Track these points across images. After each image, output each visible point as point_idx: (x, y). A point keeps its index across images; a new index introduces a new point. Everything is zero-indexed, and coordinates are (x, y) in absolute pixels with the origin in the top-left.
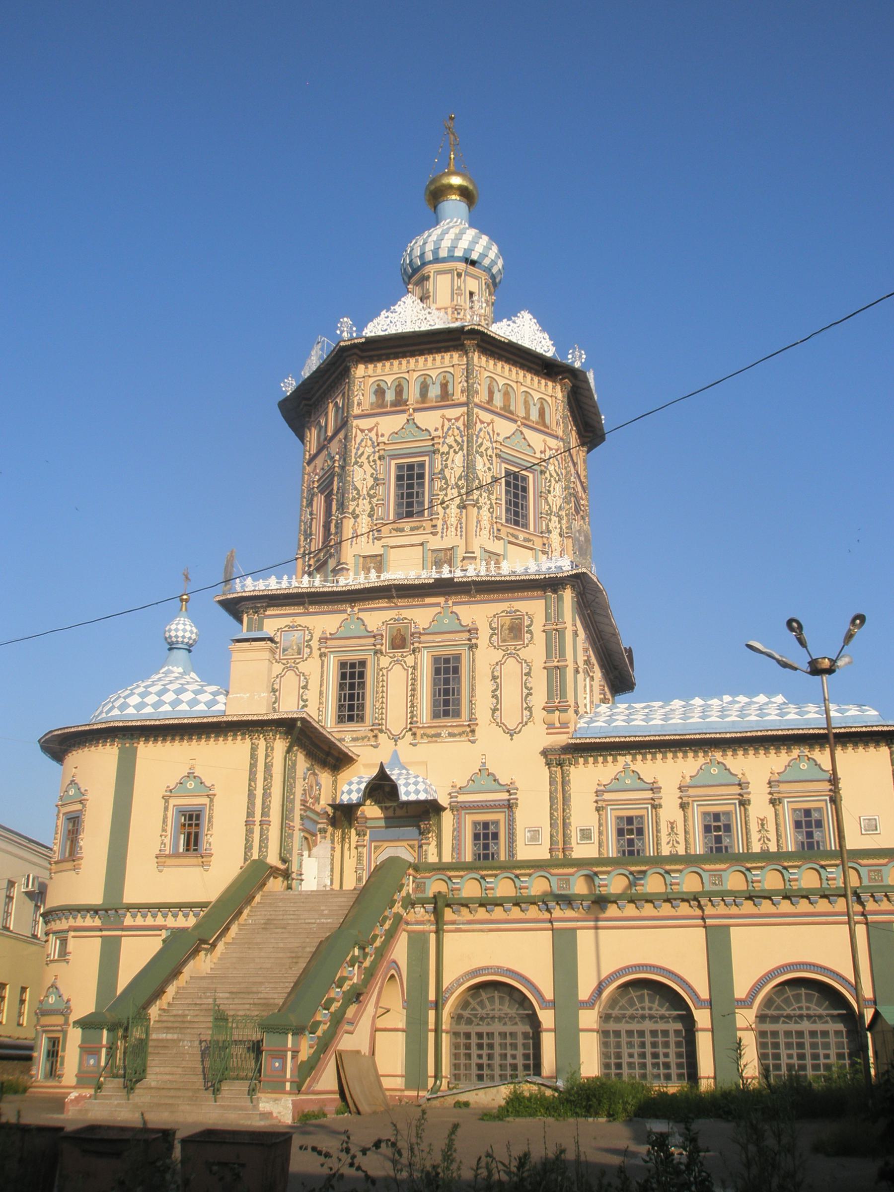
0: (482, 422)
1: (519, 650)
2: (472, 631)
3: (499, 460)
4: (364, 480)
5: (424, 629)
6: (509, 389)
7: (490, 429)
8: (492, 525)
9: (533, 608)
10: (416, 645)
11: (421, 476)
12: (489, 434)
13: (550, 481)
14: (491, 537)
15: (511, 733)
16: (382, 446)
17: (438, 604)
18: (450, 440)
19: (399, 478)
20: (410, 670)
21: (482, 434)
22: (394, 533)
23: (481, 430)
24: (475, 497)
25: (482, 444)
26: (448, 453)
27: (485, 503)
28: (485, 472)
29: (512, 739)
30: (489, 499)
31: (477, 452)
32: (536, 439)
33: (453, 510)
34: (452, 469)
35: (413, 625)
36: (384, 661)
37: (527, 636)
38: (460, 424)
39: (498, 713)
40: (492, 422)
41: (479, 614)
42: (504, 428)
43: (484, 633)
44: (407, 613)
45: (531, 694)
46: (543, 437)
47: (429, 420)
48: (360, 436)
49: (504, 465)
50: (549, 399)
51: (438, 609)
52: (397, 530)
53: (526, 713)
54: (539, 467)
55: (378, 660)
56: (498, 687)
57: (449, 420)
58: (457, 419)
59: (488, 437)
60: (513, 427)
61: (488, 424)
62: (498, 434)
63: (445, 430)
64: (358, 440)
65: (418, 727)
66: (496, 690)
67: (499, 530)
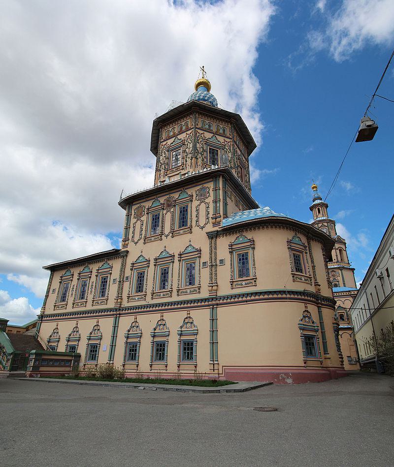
6: (211, 124)
8: (203, 164)
17: (181, 190)
32: (221, 139)
33: (189, 161)
36: (165, 212)
38: (191, 135)
41: (192, 191)
42: (208, 135)
43: (195, 196)
44: (172, 195)
47: (182, 136)
49: (209, 147)
51: (180, 192)
53: (207, 220)
54: (223, 147)
56: (198, 213)
58: (191, 133)
61: (202, 134)
67: (205, 166)
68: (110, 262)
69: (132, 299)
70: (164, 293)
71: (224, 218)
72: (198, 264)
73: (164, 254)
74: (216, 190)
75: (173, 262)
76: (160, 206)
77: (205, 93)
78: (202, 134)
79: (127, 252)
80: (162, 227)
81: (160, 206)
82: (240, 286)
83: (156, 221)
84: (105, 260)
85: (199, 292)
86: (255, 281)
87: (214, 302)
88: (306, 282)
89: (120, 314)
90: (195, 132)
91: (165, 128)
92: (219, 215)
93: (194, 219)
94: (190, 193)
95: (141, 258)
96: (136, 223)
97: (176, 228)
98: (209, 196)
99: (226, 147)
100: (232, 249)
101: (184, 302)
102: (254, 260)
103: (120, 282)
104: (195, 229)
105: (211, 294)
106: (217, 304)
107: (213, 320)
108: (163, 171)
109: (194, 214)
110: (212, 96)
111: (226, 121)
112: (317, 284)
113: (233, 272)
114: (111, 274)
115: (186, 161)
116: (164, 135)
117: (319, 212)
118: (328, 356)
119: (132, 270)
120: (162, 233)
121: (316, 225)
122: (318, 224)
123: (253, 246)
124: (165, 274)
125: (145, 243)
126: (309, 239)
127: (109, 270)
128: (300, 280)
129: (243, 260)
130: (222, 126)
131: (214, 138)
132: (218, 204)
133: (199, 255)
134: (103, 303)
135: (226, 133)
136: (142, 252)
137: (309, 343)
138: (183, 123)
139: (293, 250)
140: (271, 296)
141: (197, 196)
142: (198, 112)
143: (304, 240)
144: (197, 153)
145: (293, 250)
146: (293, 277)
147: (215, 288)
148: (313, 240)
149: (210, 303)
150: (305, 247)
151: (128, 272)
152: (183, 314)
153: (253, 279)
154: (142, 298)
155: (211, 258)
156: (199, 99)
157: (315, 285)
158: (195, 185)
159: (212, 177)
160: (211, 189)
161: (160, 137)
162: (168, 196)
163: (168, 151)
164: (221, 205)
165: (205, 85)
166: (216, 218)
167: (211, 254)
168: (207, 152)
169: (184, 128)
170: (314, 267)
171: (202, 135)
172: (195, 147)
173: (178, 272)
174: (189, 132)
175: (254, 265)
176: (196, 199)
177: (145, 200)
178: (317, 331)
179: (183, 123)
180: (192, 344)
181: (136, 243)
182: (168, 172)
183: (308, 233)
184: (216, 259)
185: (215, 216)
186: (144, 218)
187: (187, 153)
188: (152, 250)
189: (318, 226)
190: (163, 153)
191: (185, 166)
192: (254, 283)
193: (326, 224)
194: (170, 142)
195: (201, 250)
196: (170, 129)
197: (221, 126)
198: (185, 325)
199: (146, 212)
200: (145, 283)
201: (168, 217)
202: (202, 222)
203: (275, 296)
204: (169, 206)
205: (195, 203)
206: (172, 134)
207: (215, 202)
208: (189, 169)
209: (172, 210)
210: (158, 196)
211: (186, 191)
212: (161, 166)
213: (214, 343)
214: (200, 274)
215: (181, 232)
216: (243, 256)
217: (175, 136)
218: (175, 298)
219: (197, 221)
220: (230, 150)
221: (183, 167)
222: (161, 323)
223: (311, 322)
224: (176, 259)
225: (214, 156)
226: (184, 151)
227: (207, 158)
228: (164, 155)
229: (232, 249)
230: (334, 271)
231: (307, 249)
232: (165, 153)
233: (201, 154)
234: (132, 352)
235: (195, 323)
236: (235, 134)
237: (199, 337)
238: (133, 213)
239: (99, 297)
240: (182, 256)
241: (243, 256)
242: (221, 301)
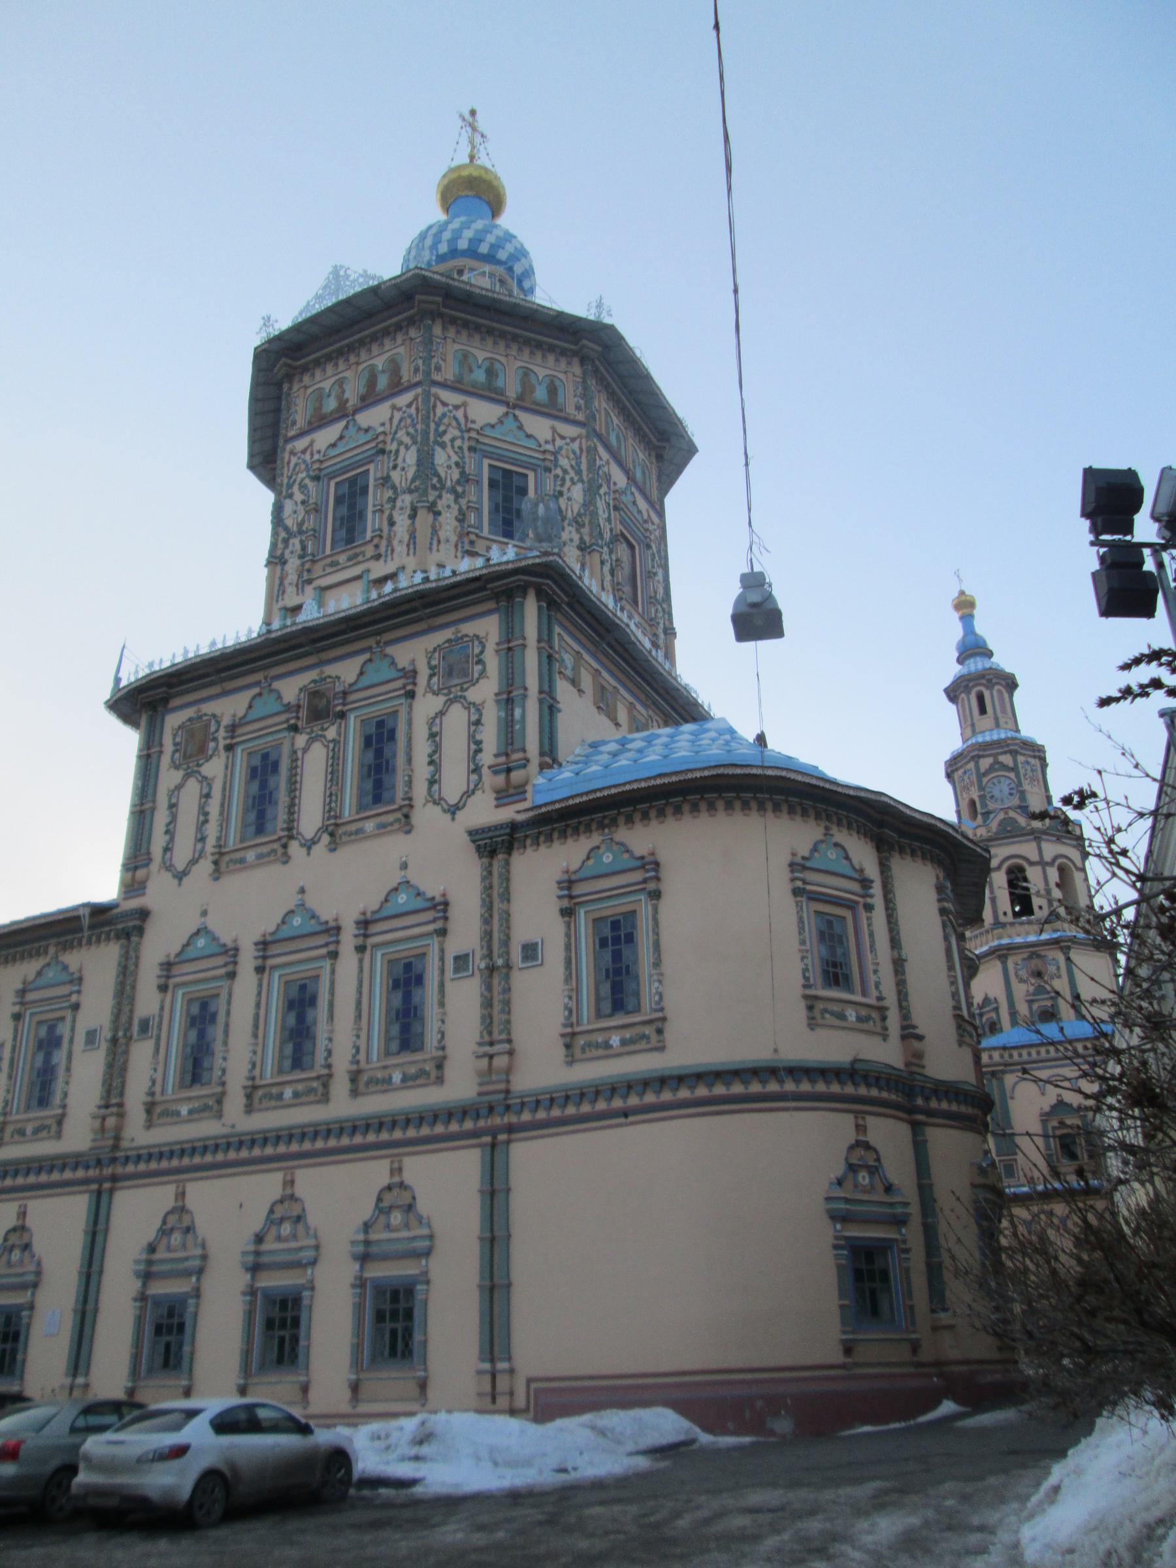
0: (445, 404)
1: (467, 689)
2: (411, 674)
3: (476, 456)
4: (295, 512)
5: (351, 685)
7: (460, 414)
8: (460, 536)
9: (487, 628)
10: (339, 708)
11: (365, 491)
12: (455, 418)
13: (563, 480)
14: (459, 554)
15: (453, 810)
16: (316, 466)
17: (369, 649)
18: (401, 435)
19: (339, 501)
20: (331, 745)
21: (446, 421)
22: (329, 570)
23: (444, 415)
24: (431, 499)
25: (445, 432)
26: (397, 451)
27: (449, 507)
28: (449, 467)
29: (453, 819)
30: (456, 501)
31: (436, 442)
32: (539, 427)
33: (402, 522)
34: (403, 469)
36: (301, 740)
37: (478, 668)
38: (413, 410)
39: (436, 787)
40: (464, 405)
41: (414, 651)
42: (483, 412)
44: (331, 670)
45: (480, 750)
46: (548, 423)
47: (375, 417)
48: (294, 460)
49: (486, 462)
50: (561, 376)
51: (367, 656)
52: (332, 564)
53: (474, 777)
55: (293, 738)
56: (437, 749)
57: (399, 409)
58: (409, 405)
59: (454, 423)
60: (499, 410)
61: (457, 407)
62: (473, 422)
63: (396, 421)
64: (292, 465)
65: (337, 825)
66: (435, 752)
67: (472, 543)
68: (73, 959)
69: (166, 1113)
70: (300, 1087)
71: (543, 766)
72: (437, 963)
73: (297, 921)
74: (510, 649)
75: (334, 955)
76: (283, 717)
77: (479, 225)
78: (457, 407)
79: (144, 914)
80: (292, 805)
81: (283, 717)
82: (601, 1052)
83: (266, 775)
84: (52, 950)
85: (440, 1080)
86: (660, 1031)
87: (497, 1121)
88: (865, 1026)
89: (114, 1178)
90: (427, 399)
91: (306, 379)
92: (520, 755)
93: (422, 772)
94: (403, 662)
95: (201, 942)
96: (179, 787)
97: (348, 810)
98: (483, 673)
99: (564, 462)
100: (571, 897)
101: (380, 1123)
102: (657, 945)
103: (114, 1041)
104: (426, 816)
105: (490, 1088)
106: (510, 1129)
107: (495, 1193)
108: (293, 564)
109: (422, 749)
110: (509, 237)
111: (563, 353)
112: (910, 1034)
113: (574, 993)
114: (76, 1007)
115: (392, 523)
116: (300, 411)
117: (983, 711)
118: (944, 1318)
119: (163, 988)
120: (291, 832)
121: (971, 765)
122: (976, 758)
123: (651, 886)
124: (301, 1000)
125: (217, 873)
126: (883, 847)
127: (65, 990)
128: (837, 1022)
129: (617, 938)
130: (544, 369)
131: (510, 423)
132: (518, 712)
133: (439, 925)
134: (44, 1134)
135: (560, 400)
136: (204, 913)
137: (867, 1275)
138: (380, 362)
139: (814, 897)
140: (720, 1090)
141: (431, 676)
142: (441, 315)
143: (863, 855)
144: (434, 487)
145: (814, 897)
146: (810, 1008)
147: (501, 1062)
148: (902, 851)
149: (481, 1123)
150: (866, 883)
151: (147, 1001)
152: (377, 1172)
153: (650, 1022)
154: (206, 1108)
155: (488, 936)
156: (454, 253)
157: (904, 1038)
158: (423, 625)
159: (496, 596)
160: (491, 647)
161: (284, 415)
162: (313, 675)
163: (317, 478)
164: (531, 712)
165: (474, 191)
166: (509, 770)
167: (487, 920)
168: (478, 483)
169: (382, 382)
170: (899, 965)
171: (460, 414)
172: (425, 463)
173: (353, 996)
174: (403, 400)
175: (657, 964)
177: (216, 690)
178: (900, 1221)
179: (380, 362)
180: (410, 1292)
181: (180, 876)
182: (318, 570)
183: (881, 824)
184: (506, 942)
185: (503, 759)
186: (214, 768)
187: (394, 487)
188: (248, 906)
189: (977, 767)
190: (296, 489)
191: (384, 543)
192: (654, 1038)
193: (1007, 759)
194: (325, 437)
195: (446, 904)
196: (326, 385)
197: (541, 372)
198: (382, 1218)
199: (222, 743)
200: (218, 1047)
201: (315, 762)
202: (454, 783)
203: (737, 1089)
205: (426, 705)
206: (331, 405)
207: (509, 699)
208: (401, 556)
209: (331, 733)
210: (274, 671)
211: (389, 650)
212: (286, 542)
213: (495, 1289)
214: (442, 1004)
215: (369, 826)
216: (615, 925)
217: (343, 413)
218: (342, 1105)
220: (579, 472)
221: (377, 546)
222: (287, 1212)
223: (880, 1188)
224: (348, 940)
225: (507, 499)
226: (386, 481)
227: (478, 511)
228: (299, 497)
229: (571, 897)
230: (1039, 956)
231: (877, 889)
232: (303, 487)
233: (453, 490)
234: (167, 1336)
235: (422, 1207)
236: (601, 403)
237: (437, 1266)
238: (168, 747)
239: (28, 1108)
240: (374, 929)
241: (615, 925)
242: (526, 1116)
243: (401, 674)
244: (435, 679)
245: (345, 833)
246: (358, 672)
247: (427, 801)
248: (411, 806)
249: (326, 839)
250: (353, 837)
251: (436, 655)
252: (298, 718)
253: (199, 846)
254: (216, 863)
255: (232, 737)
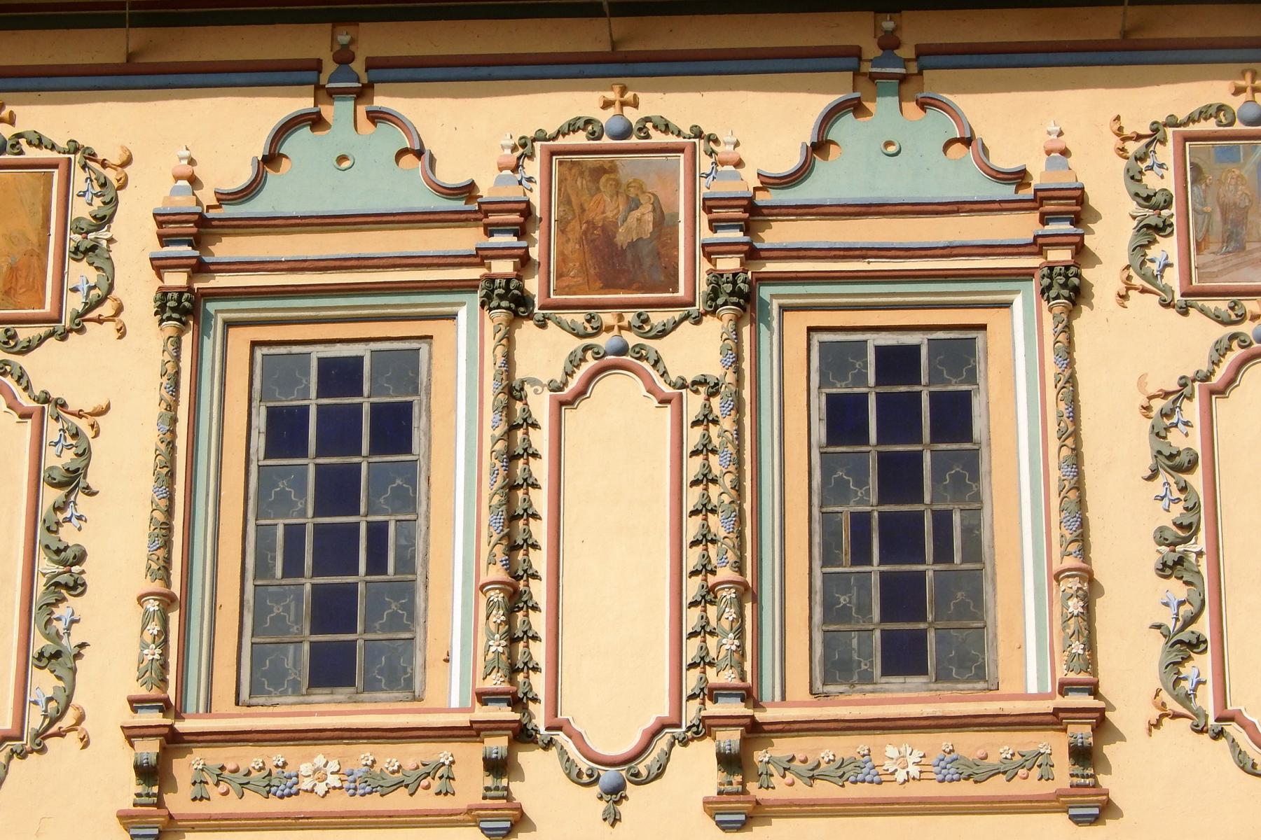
5: (769, 182)
10: (730, 264)
20: (694, 404)
35: (705, 164)
36: (543, 351)
39: (1201, 665)
66: (1188, 529)
141: (1152, 231)
162: (584, 101)
176: (1141, 277)
177: (105, 47)
204: (625, 266)
205: (1136, 343)
215: (901, 757)
219: (1184, 646)
243: (1007, 192)
244: (1167, 248)
245: (787, 767)
246: (807, 135)
247: (1167, 715)
248: (1101, 723)
249: (696, 770)
250: (824, 790)
251: (1165, 153)
252: (524, 262)
253: (44, 683)
254: (149, 773)
255: (200, 268)
